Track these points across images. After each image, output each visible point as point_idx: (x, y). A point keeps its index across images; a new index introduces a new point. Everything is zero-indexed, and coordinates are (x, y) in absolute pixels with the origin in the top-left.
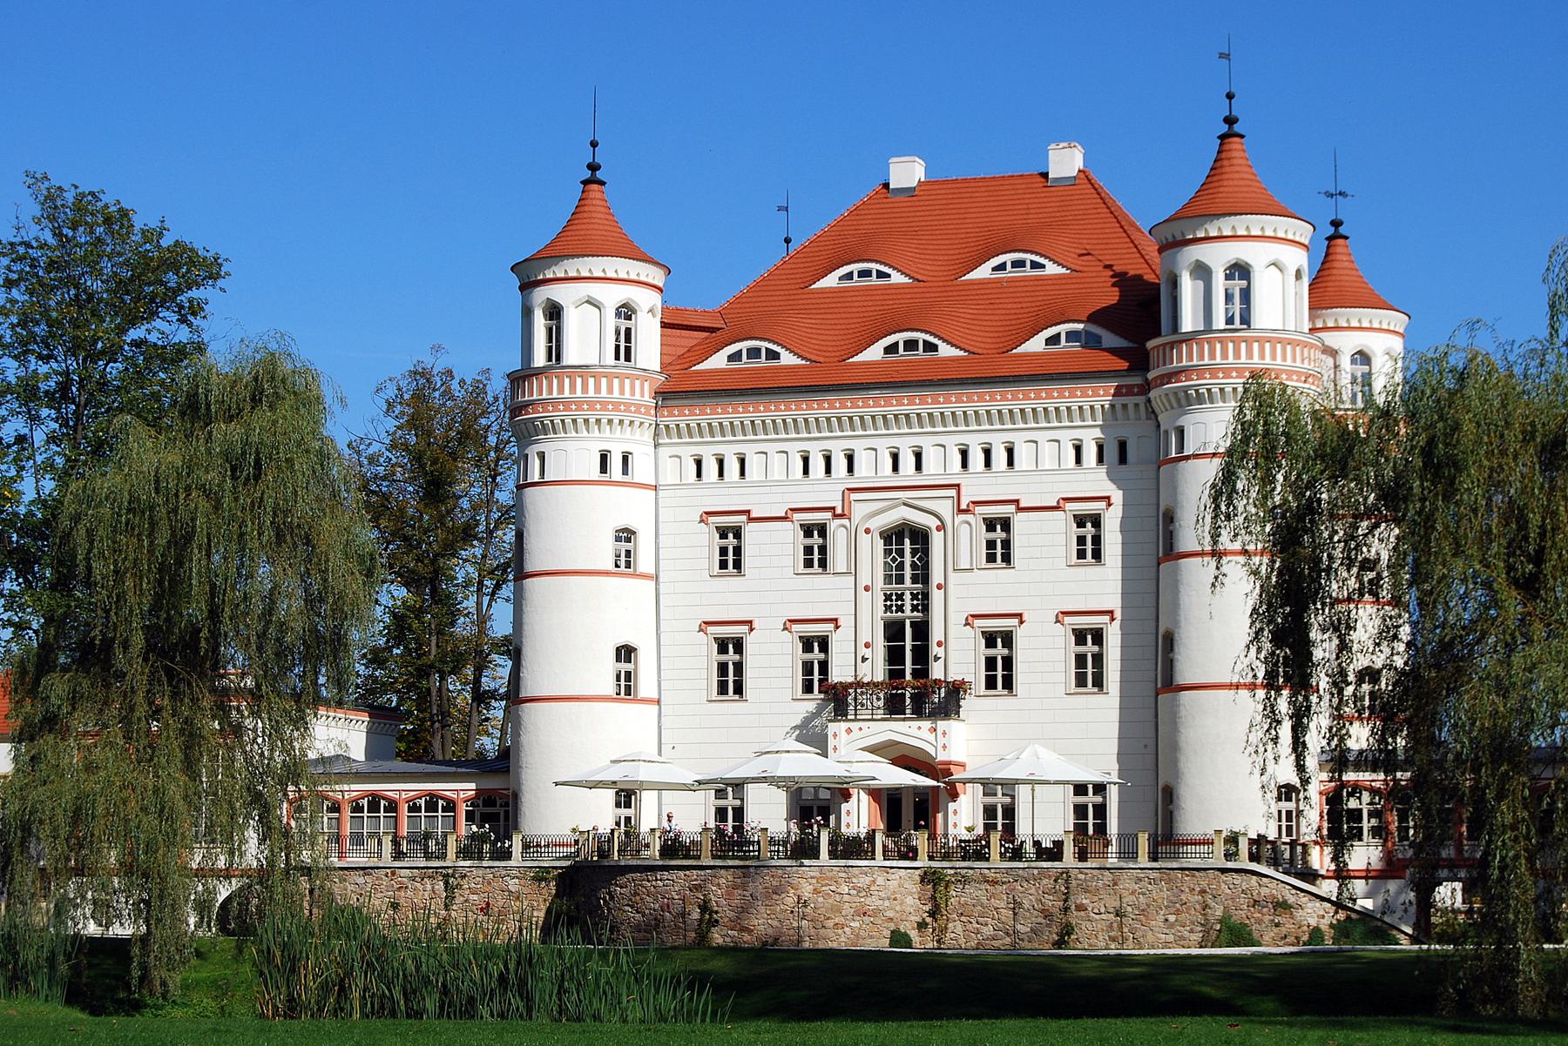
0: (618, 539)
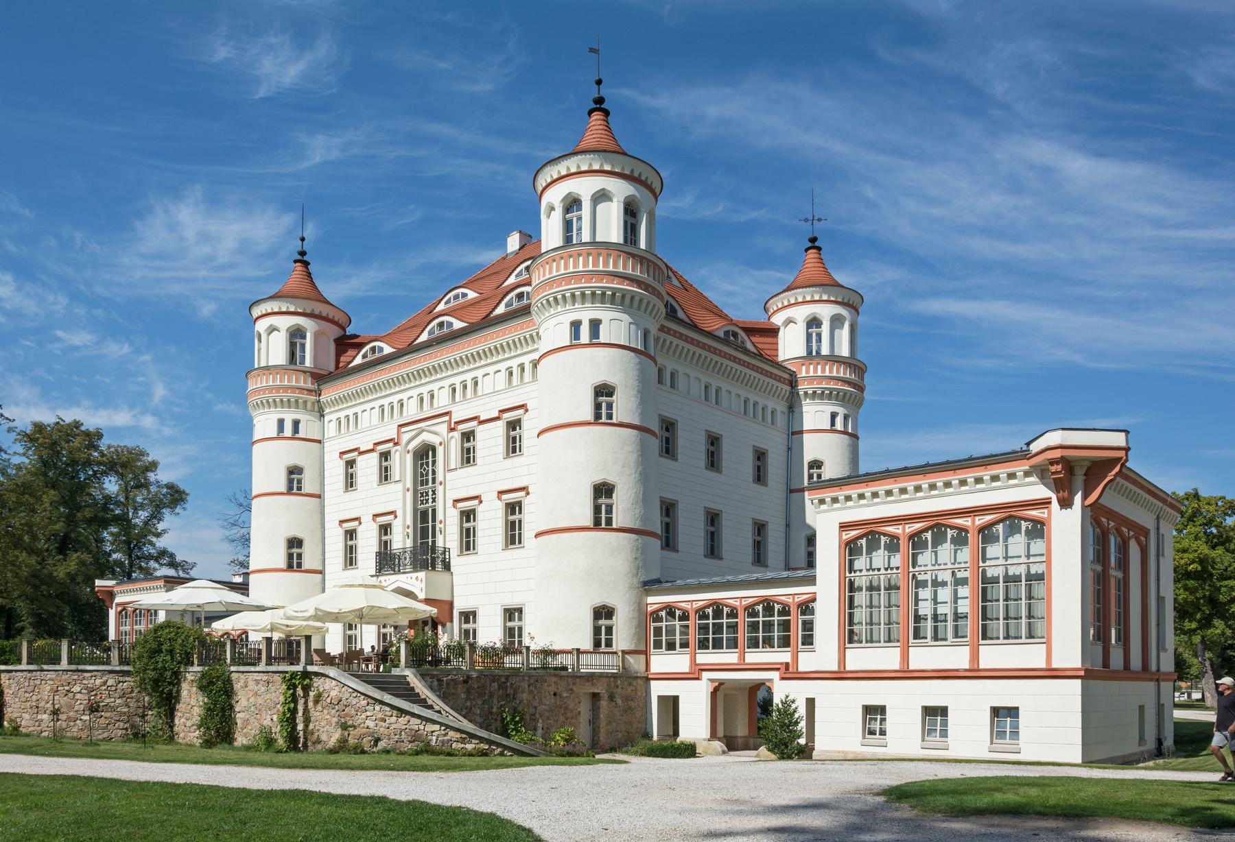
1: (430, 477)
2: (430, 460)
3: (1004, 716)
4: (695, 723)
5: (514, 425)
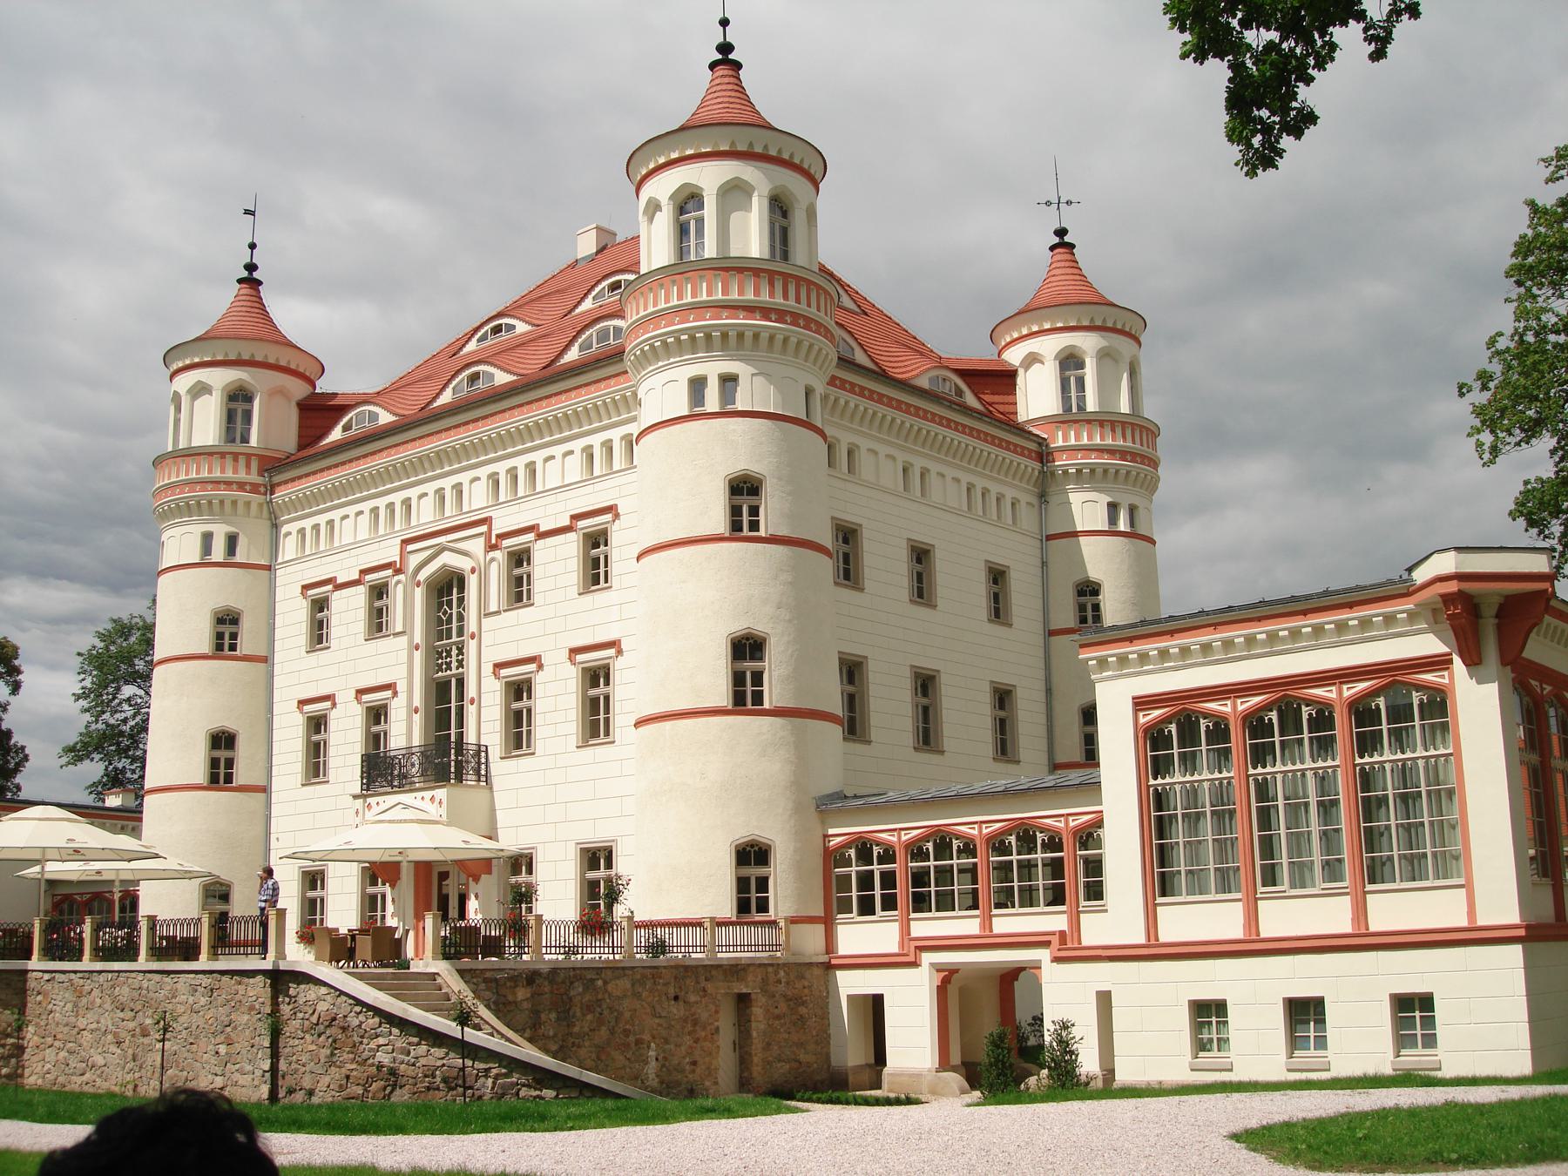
0: (220, 621)
1: (454, 625)
2: (455, 597)
3: (1412, 1011)
4: (912, 1041)
5: (597, 540)
